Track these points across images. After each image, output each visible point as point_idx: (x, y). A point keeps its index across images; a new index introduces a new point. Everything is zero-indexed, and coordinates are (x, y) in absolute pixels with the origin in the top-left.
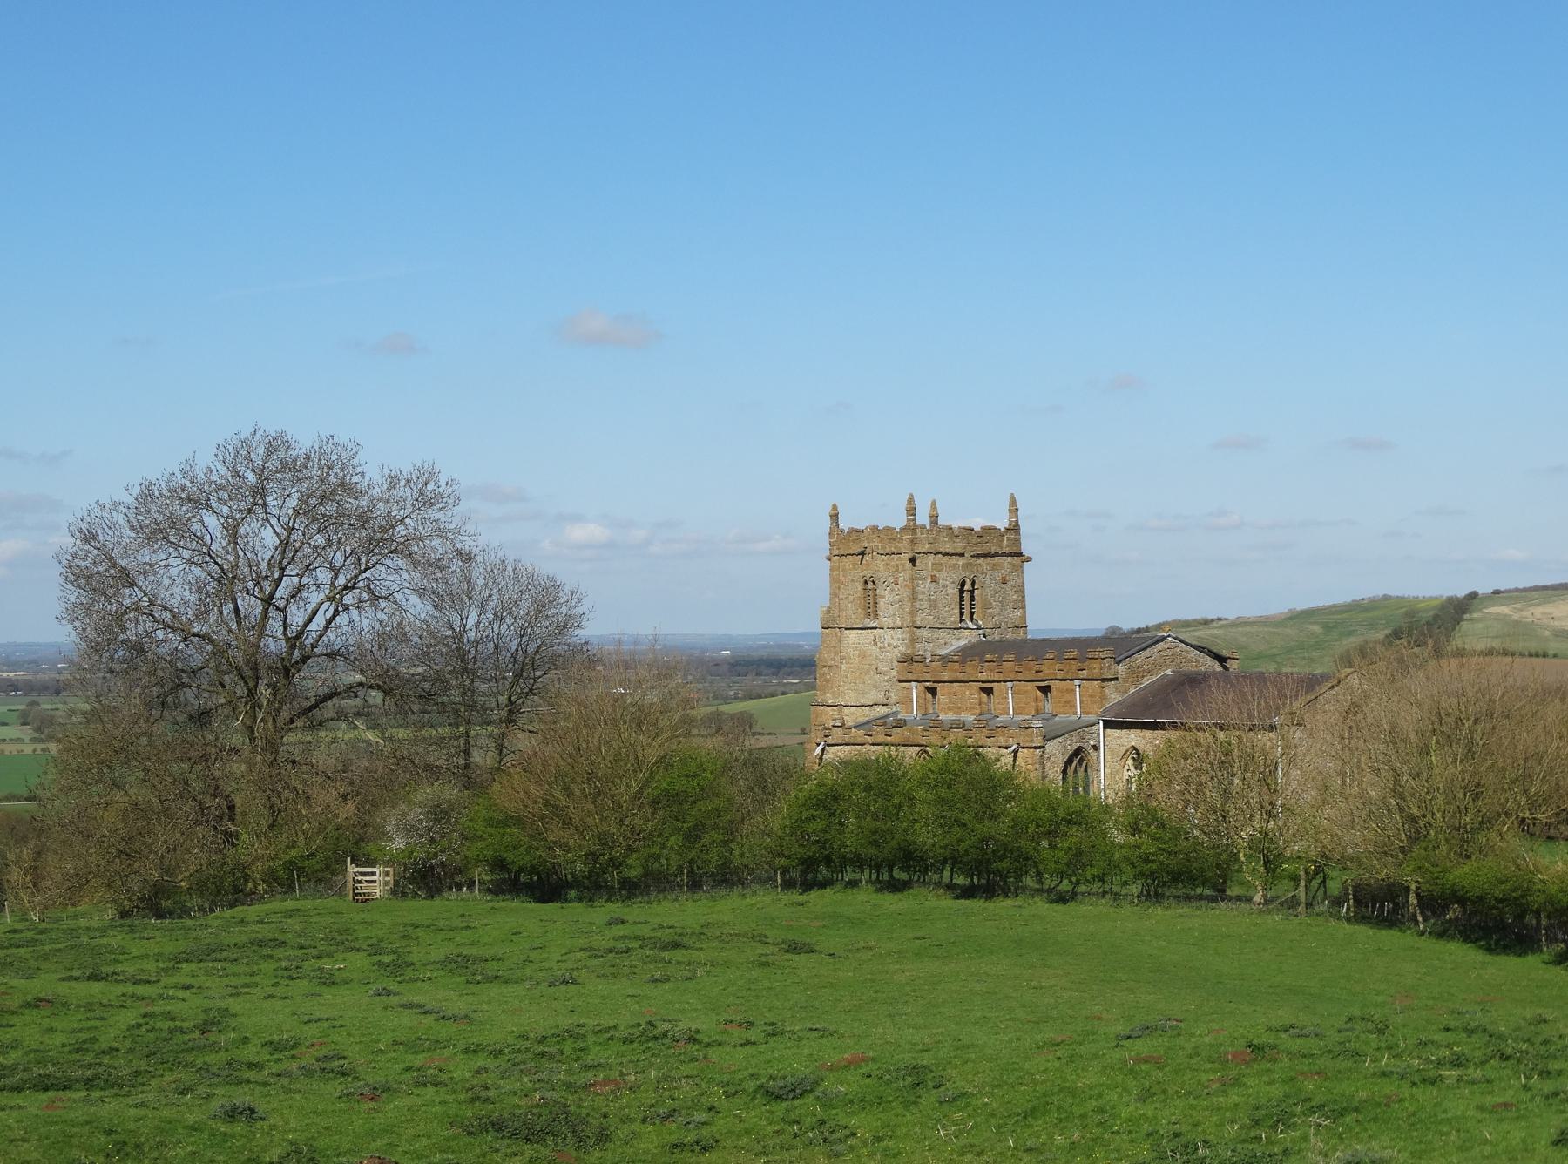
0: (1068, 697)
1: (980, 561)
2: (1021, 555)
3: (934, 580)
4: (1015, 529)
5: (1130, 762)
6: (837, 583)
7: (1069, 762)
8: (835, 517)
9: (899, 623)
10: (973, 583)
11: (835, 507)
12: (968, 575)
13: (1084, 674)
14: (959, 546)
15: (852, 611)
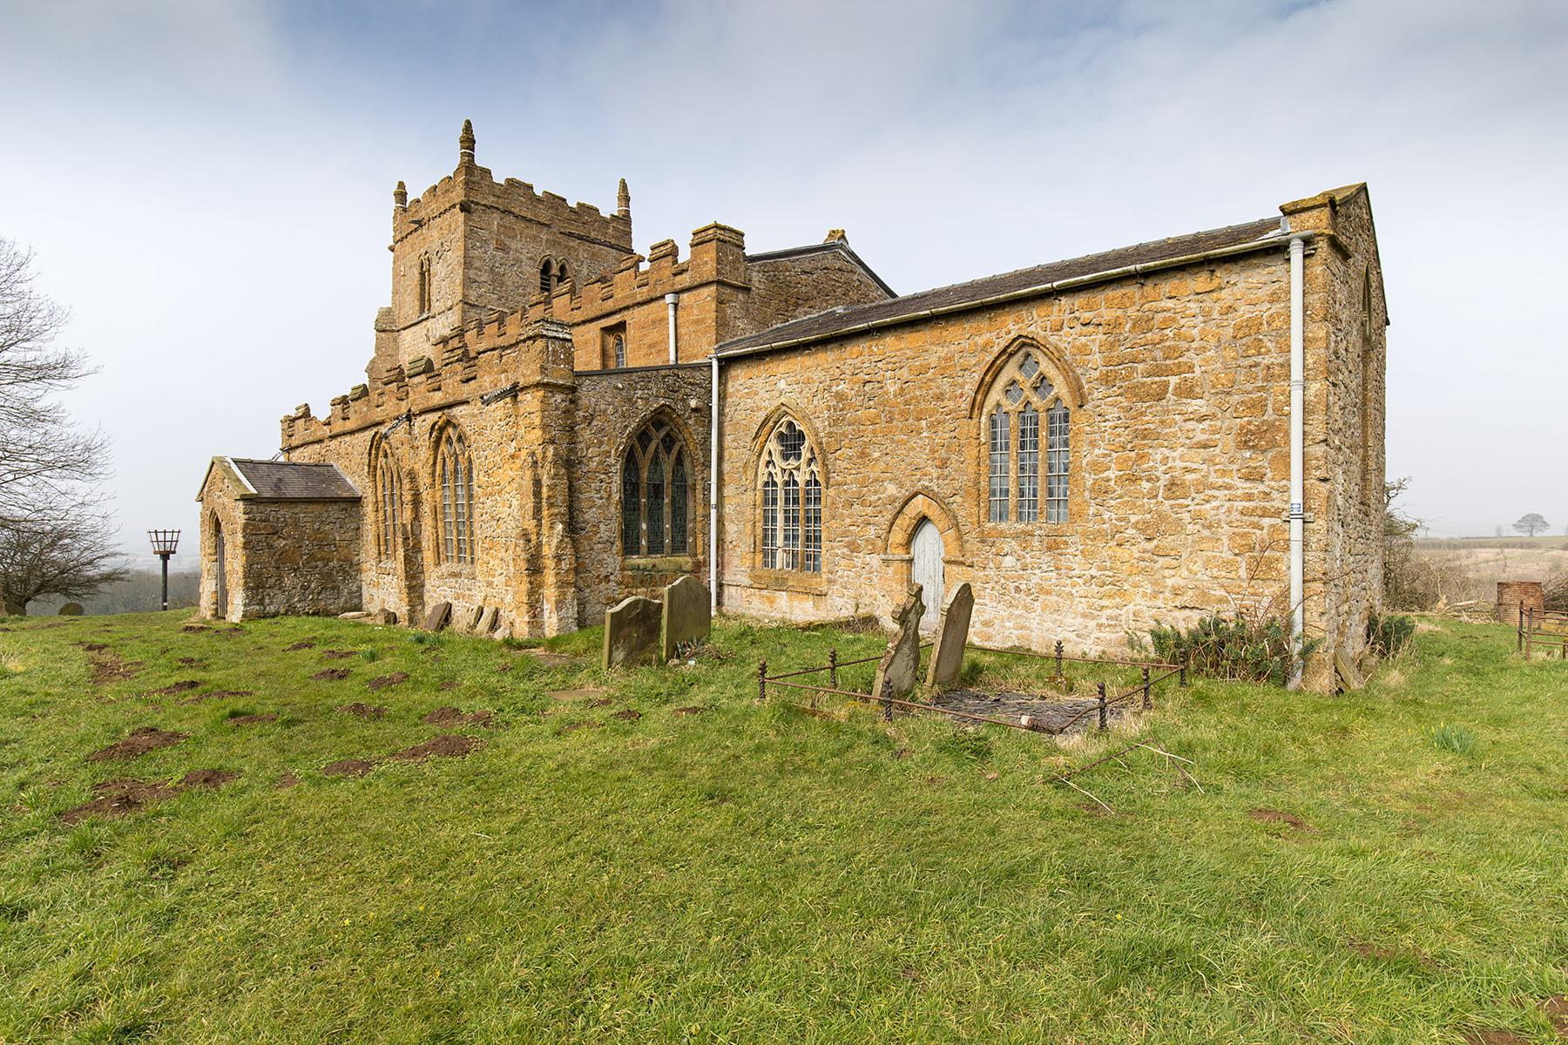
0: (654, 336)
1: (574, 243)
2: (631, 251)
3: (501, 247)
4: (625, 220)
5: (773, 446)
6: (398, 276)
7: (642, 437)
8: (401, 195)
9: (449, 303)
10: (562, 269)
11: (401, 185)
12: (557, 257)
13: (685, 281)
14: (544, 215)
15: (411, 309)
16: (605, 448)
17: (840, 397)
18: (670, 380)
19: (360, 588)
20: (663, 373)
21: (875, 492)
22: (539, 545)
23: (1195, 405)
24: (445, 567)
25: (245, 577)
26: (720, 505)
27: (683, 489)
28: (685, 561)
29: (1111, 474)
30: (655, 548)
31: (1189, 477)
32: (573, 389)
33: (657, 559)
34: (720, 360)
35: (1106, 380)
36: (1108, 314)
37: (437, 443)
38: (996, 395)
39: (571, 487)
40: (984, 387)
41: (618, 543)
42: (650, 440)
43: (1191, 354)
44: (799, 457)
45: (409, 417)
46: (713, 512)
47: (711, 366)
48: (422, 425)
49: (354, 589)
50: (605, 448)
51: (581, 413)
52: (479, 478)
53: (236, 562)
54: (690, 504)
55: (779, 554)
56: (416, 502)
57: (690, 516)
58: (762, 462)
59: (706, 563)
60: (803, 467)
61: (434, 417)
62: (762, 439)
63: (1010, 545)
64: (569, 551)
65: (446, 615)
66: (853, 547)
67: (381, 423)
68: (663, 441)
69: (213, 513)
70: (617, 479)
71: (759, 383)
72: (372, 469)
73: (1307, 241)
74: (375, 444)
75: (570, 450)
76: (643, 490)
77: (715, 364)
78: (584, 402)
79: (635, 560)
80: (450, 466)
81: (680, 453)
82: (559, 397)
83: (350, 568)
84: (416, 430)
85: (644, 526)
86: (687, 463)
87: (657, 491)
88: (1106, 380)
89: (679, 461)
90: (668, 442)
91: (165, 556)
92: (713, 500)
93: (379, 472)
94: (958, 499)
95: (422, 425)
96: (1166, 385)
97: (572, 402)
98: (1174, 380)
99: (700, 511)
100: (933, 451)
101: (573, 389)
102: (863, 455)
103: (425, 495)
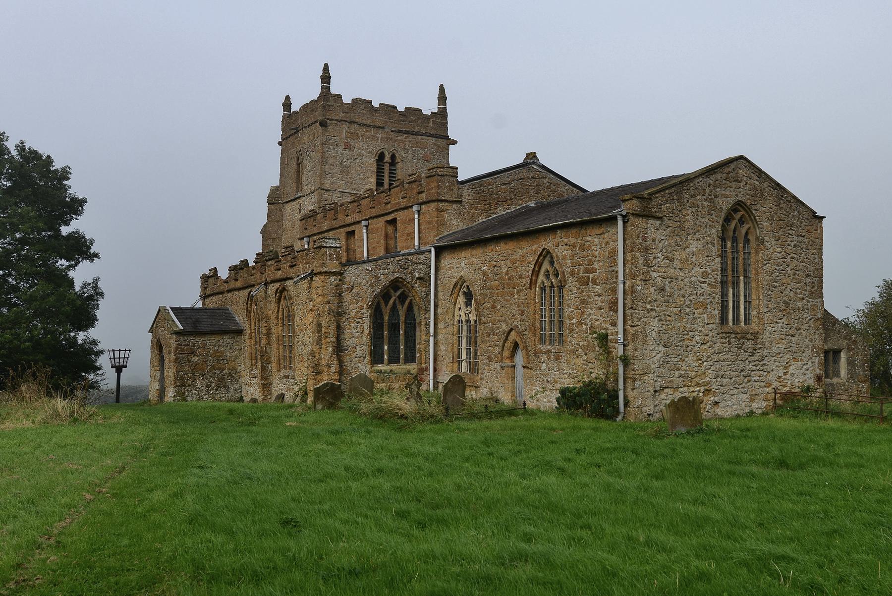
5: (461, 299)
7: (385, 295)
16: (360, 304)
17: (485, 274)
18: (402, 263)
19: (241, 387)
20: (398, 259)
21: (498, 328)
22: (320, 359)
23: (598, 288)
24: (284, 372)
25: (175, 379)
26: (435, 334)
27: (412, 326)
28: (413, 368)
29: (574, 321)
30: (394, 360)
31: (597, 323)
32: (341, 274)
33: (394, 367)
34: (435, 248)
35: (572, 273)
36: (572, 240)
37: (279, 300)
38: (541, 277)
39: (339, 328)
40: (536, 273)
41: (368, 358)
42: (390, 298)
43: (595, 263)
44: (471, 305)
45: (267, 284)
46: (432, 338)
47: (430, 251)
48: (272, 288)
49: (237, 387)
50: (360, 304)
51: (346, 286)
52: (297, 321)
53: (170, 372)
54: (418, 333)
55: (464, 364)
56: (269, 334)
57: (418, 341)
58: (457, 309)
59: (427, 369)
60: (473, 312)
61: (277, 285)
62: (455, 295)
63: (544, 358)
64: (336, 362)
65: (282, 397)
66: (490, 359)
67: (253, 286)
68: (399, 297)
69: (159, 341)
70: (367, 321)
71: (454, 262)
72: (249, 313)
73: (624, 217)
74: (250, 297)
75: (338, 307)
76: (385, 327)
77: (433, 250)
78: (347, 279)
79: (380, 367)
80: (286, 314)
81: (411, 304)
82: (333, 278)
83: (234, 374)
84: (269, 292)
85: (386, 348)
86: (415, 309)
87: (394, 328)
88: (572, 273)
89: (410, 308)
90: (403, 298)
91: (119, 369)
92: (432, 331)
93: (252, 314)
94: (527, 332)
95: (272, 288)
96: (588, 277)
97: (340, 280)
98: (591, 275)
99: (423, 337)
100: (519, 306)
101: (341, 274)
102: (494, 307)
103: (274, 330)
